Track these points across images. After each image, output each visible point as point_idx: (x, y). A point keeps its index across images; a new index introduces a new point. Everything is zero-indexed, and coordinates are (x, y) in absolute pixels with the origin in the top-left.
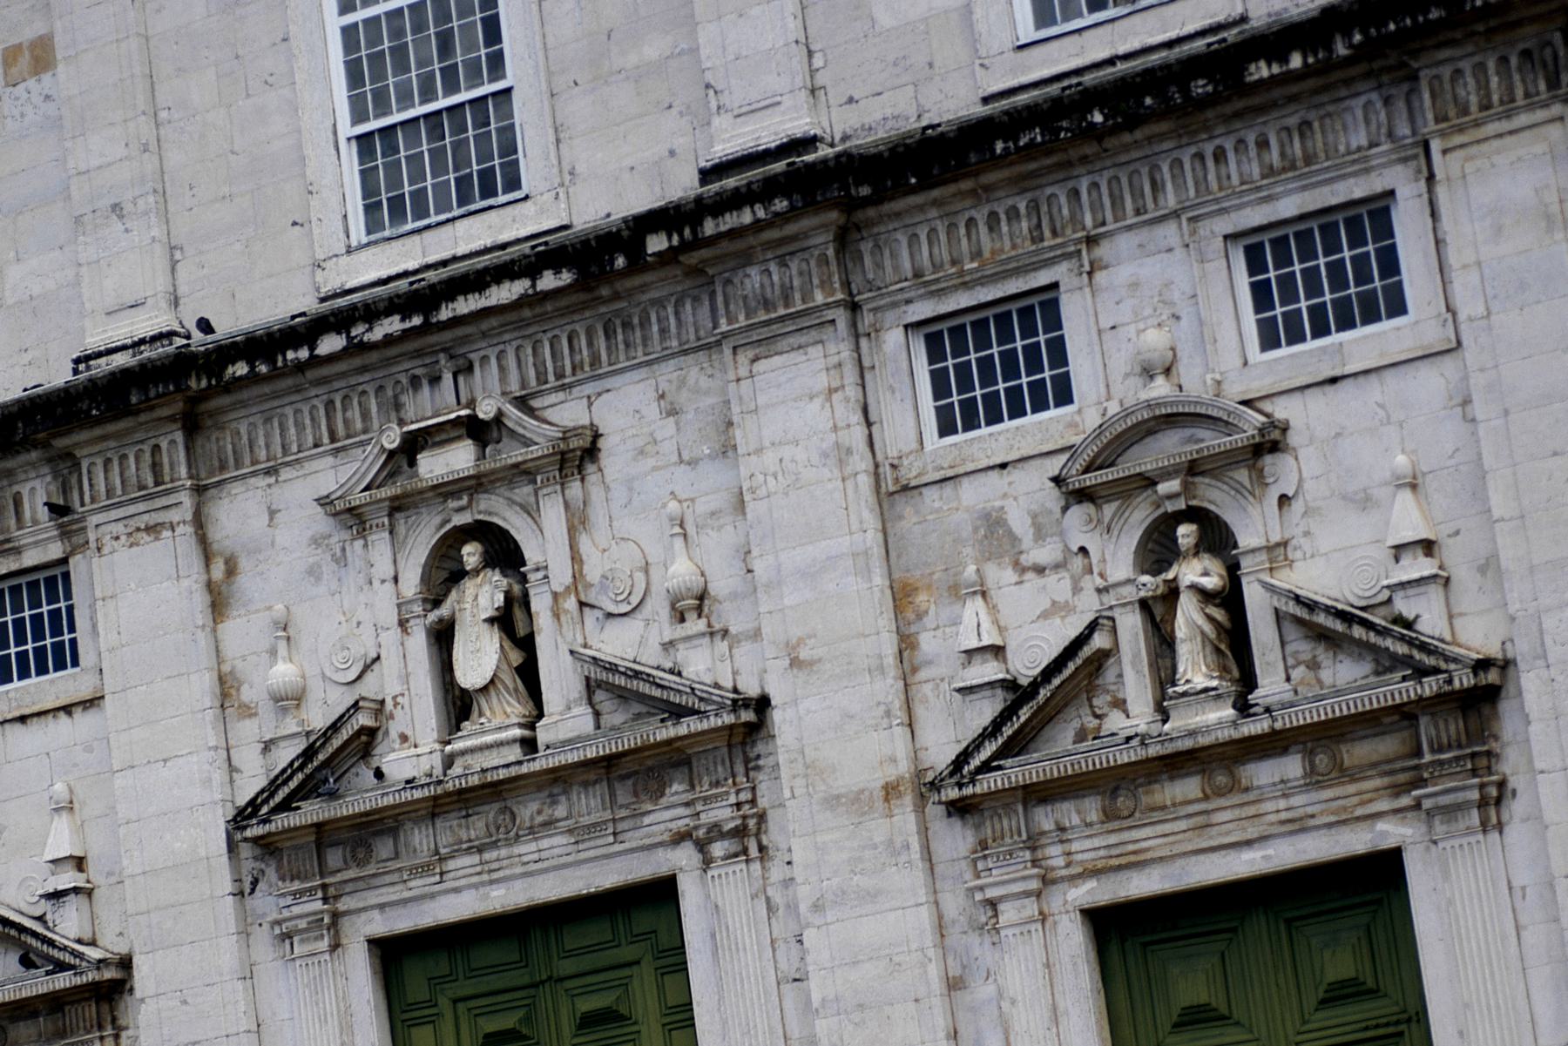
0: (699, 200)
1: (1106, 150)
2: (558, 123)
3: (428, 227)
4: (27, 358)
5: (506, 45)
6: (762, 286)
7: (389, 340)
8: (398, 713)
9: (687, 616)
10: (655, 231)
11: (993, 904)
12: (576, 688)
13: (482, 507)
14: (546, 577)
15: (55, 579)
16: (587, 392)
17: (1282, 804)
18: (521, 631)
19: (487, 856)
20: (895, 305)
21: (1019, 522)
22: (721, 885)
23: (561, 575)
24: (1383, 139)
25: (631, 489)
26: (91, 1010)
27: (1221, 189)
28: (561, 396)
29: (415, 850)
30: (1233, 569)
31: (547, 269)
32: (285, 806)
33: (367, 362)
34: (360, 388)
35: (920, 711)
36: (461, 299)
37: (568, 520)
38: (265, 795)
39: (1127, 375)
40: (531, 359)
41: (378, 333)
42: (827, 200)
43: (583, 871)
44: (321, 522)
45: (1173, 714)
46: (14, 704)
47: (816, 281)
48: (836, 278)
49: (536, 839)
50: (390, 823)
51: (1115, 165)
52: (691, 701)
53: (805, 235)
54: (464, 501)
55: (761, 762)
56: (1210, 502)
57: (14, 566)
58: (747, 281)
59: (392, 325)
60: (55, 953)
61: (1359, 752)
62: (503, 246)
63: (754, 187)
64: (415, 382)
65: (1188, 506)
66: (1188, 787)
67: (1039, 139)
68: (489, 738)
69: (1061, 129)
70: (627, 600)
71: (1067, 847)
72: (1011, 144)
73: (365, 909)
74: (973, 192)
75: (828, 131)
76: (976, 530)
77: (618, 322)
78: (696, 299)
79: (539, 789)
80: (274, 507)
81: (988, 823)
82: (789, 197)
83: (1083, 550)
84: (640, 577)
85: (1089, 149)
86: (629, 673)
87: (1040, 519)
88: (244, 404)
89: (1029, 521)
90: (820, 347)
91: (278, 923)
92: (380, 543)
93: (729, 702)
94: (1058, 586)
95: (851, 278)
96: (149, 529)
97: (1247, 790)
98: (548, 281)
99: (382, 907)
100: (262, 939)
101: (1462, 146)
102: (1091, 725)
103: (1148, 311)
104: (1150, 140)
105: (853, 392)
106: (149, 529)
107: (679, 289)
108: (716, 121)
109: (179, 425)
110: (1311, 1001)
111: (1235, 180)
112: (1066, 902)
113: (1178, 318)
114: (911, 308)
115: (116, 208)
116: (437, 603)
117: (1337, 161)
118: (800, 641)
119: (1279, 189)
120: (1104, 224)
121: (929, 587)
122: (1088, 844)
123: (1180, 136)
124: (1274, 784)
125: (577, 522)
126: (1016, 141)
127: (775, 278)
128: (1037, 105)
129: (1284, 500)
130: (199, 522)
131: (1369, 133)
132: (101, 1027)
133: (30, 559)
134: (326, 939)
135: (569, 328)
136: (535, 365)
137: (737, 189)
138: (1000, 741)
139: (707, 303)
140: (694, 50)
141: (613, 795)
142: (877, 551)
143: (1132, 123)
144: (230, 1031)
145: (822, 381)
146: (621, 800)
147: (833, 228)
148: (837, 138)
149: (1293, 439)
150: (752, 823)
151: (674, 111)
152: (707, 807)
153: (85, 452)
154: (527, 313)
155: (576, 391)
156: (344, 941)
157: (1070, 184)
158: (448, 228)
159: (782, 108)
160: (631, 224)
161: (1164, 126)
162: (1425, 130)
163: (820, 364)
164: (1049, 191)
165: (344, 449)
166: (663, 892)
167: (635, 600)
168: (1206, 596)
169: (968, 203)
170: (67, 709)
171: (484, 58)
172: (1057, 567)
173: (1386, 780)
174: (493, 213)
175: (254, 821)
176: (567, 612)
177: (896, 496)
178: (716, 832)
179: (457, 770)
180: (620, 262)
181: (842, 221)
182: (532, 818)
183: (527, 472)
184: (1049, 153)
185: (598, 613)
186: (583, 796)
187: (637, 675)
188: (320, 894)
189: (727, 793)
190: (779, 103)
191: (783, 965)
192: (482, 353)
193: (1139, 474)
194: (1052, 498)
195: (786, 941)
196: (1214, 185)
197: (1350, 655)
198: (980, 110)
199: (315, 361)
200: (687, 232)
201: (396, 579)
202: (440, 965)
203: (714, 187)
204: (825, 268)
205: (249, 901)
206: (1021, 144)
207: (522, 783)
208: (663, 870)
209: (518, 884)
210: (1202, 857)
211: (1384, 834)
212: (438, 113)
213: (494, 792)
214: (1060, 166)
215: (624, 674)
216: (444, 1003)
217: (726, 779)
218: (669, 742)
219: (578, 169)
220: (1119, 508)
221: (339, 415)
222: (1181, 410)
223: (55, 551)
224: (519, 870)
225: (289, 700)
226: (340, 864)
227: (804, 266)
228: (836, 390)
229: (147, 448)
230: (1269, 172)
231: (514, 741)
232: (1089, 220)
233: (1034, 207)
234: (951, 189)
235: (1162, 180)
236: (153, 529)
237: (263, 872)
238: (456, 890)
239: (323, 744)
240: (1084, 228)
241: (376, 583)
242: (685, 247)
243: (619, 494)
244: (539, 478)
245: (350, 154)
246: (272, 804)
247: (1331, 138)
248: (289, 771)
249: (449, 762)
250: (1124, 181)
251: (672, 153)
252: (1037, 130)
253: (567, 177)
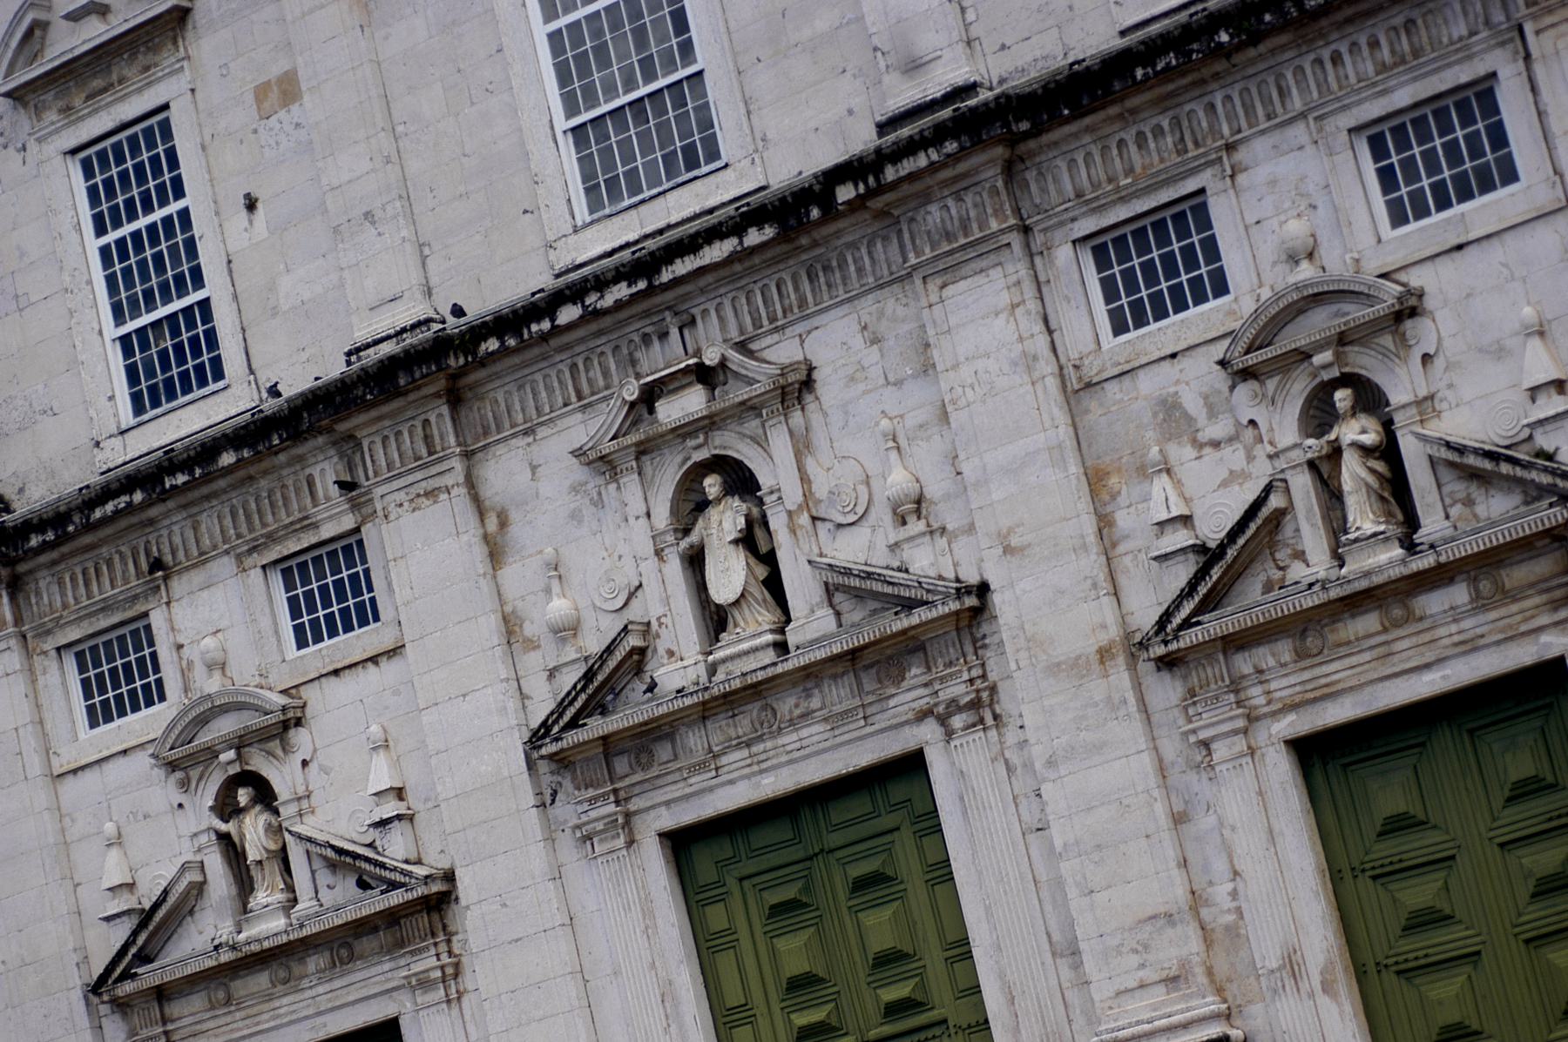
0: (878, 151)
1: (1234, 66)
2: (747, 96)
3: (643, 202)
4: (304, 356)
5: (694, 33)
6: (943, 221)
7: (619, 305)
8: (663, 631)
9: (908, 519)
10: (843, 182)
11: (1205, 744)
12: (817, 593)
13: (717, 442)
14: (780, 498)
15: (350, 547)
16: (798, 332)
17: (1454, 628)
18: (764, 549)
19: (755, 749)
20: (1062, 224)
21: (1192, 403)
22: (963, 753)
23: (793, 494)
24: (1481, 27)
25: (846, 413)
26: (423, 920)
27: (1341, 88)
28: (776, 337)
29: (691, 751)
30: (1388, 425)
31: (751, 226)
32: (573, 724)
33: (602, 326)
34: (599, 350)
35: (1122, 581)
36: (678, 261)
37: (793, 446)
39: (1274, 263)
40: (746, 308)
41: (609, 300)
42: (992, 138)
43: (842, 753)
44: (578, 472)
45: (1348, 559)
46: (327, 660)
47: (989, 211)
48: (1007, 206)
49: (797, 730)
50: (667, 729)
51: (1244, 78)
53: (976, 171)
54: (701, 439)
55: (987, 641)
56: (1361, 368)
57: (314, 540)
58: (929, 218)
59: (621, 291)
60: (387, 874)
61: (1517, 575)
62: (711, 211)
63: (926, 133)
64: (646, 340)
65: (1342, 374)
66: (1369, 622)
67: (1174, 62)
68: (745, 646)
69: (1192, 51)
70: (853, 511)
71: (1266, 687)
72: (1149, 70)
73: (653, 807)
74: (1120, 116)
75: (986, 76)
76: (1155, 415)
77: (819, 267)
78: (885, 239)
79: (794, 685)
80: (534, 463)
81: (1194, 673)
82: (956, 137)
83: (1252, 422)
84: (862, 489)
85: (1220, 66)
87: (1211, 399)
88: (498, 376)
89: (1202, 402)
90: (999, 269)
91: (578, 827)
92: (631, 482)
93: (953, 591)
94: (1234, 457)
95: (1020, 204)
96: (427, 494)
97: (1421, 619)
98: (753, 237)
99: (667, 803)
100: (566, 842)
101: (1553, 26)
102: (1276, 577)
103: (1287, 204)
104: (1273, 52)
105: (1033, 305)
106: (427, 494)
107: (869, 231)
108: (887, 79)
109: (444, 400)
110: (1498, 802)
111: (1353, 79)
112: (1270, 735)
113: (1315, 207)
114: (1076, 225)
115: (368, 215)
116: (687, 532)
117: (1442, 52)
118: (1010, 531)
119: (1393, 82)
120: (1239, 131)
121: (1119, 470)
122: (1285, 682)
123: (1299, 45)
124: (1445, 612)
125: (802, 446)
126: (1154, 66)
127: (954, 212)
128: (1168, 33)
129: (1426, 358)
130: (471, 483)
131: (1467, 24)
132: (433, 935)
133: (327, 532)
134: (622, 836)
135: (777, 276)
136: (750, 312)
137: (911, 137)
138: (1197, 599)
139: (895, 241)
140: (860, 19)
141: (860, 684)
142: (1070, 444)
143: (1255, 39)
144: (546, 927)
145: (1005, 298)
146: (867, 687)
147: (1000, 162)
148: (995, 83)
149: (1429, 303)
150: (985, 695)
151: (848, 74)
153: (365, 433)
154: (738, 267)
155: (788, 331)
156: (638, 837)
157: (1206, 99)
158: (660, 201)
159: (943, 60)
160: (821, 179)
161: (1283, 39)
162: (1519, 15)
163: (1001, 283)
164: (1187, 108)
165: (590, 405)
166: (913, 764)
167: (860, 510)
168: (1366, 451)
169: (1116, 127)
170: (374, 660)
171: (675, 47)
172: (1231, 440)
173: (1545, 597)
174: (698, 183)
175: (548, 740)
176: (802, 527)
177: (1082, 393)
178: (954, 706)
179: (720, 676)
180: (815, 213)
181: (1007, 156)
182: (791, 712)
183: (753, 408)
184: (1183, 74)
185: (829, 525)
187: (869, 575)
188: (612, 798)
189: (960, 671)
190: (940, 57)
191: (1026, 816)
192: (702, 307)
193: (1295, 350)
194: (1220, 379)
195: (1026, 796)
196: (1334, 86)
197: (1501, 490)
198: (1119, 43)
199: (556, 330)
200: (871, 180)
201: (648, 515)
202: (723, 849)
203: (891, 138)
204: (996, 199)
205: (551, 811)
206: (1159, 68)
207: (779, 681)
208: (911, 745)
209: (785, 771)
210: (1387, 684)
211: (1548, 645)
212: (641, 99)
213: (755, 692)
214: (1194, 84)
215: (858, 576)
216: (732, 883)
218: (904, 632)
219: (769, 136)
220: (1280, 382)
221: (583, 375)
222: (1326, 289)
223: (348, 522)
224: (784, 758)
225: (567, 631)
226: (627, 769)
227: (978, 199)
228: (1018, 305)
229: (418, 423)
230: (1382, 68)
231: (768, 645)
232: (1226, 130)
233: (1176, 123)
234: (1101, 115)
235: (1288, 87)
236: (430, 494)
238: (731, 782)
239: (601, 666)
240: (1222, 137)
241: (632, 520)
242: (871, 194)
243: (836, 418)
244: (764, 412)
245: (567, 146)
246: (561, 723)
247: (1434, 31)
249: (712, 670)
250: (1254, 90)
251: (850, 112)
252: (1172, 55)
253: (760, 144)
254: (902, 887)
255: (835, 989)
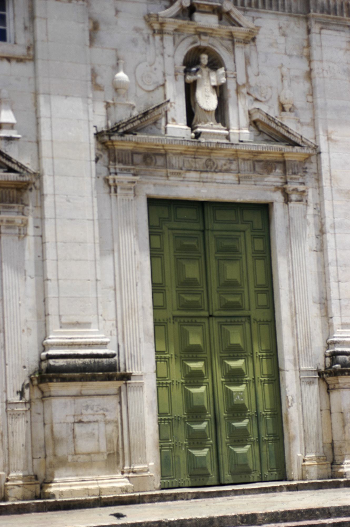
38: (124, 125)
52: (299, 141)
86: (279, 124)
93: (313, 146)
125: (247, 62)
152: (291, 181)
155: (249, 13)
156: (137, 194)
175: (117, 134)
176: (243, 93)
178: (295, 190)
182: (222, 167)
186: (243, 164)
217: (298, 173)
237: (101, 156)
241: (166, 56)
246: (125, 129)
248: (136, 118)
254: (240, 256)
255: (201, 289)
